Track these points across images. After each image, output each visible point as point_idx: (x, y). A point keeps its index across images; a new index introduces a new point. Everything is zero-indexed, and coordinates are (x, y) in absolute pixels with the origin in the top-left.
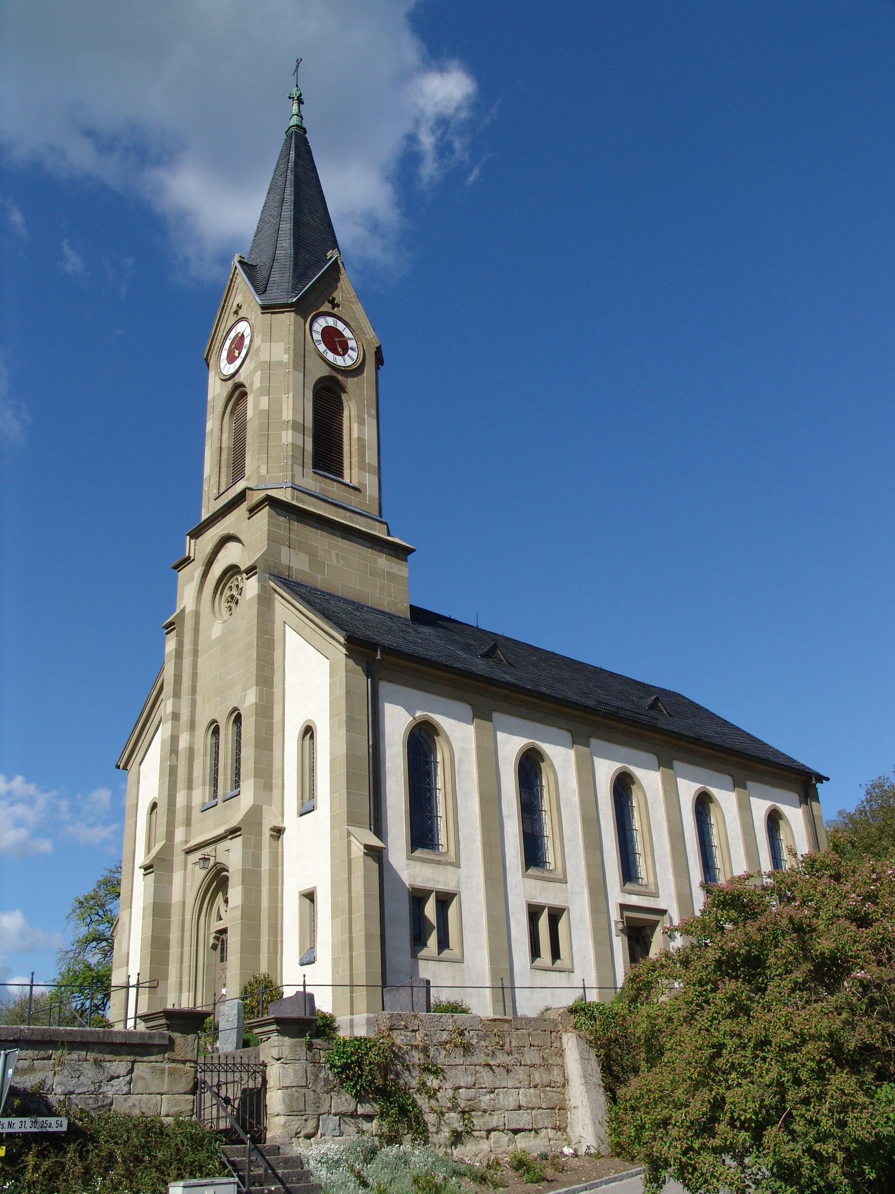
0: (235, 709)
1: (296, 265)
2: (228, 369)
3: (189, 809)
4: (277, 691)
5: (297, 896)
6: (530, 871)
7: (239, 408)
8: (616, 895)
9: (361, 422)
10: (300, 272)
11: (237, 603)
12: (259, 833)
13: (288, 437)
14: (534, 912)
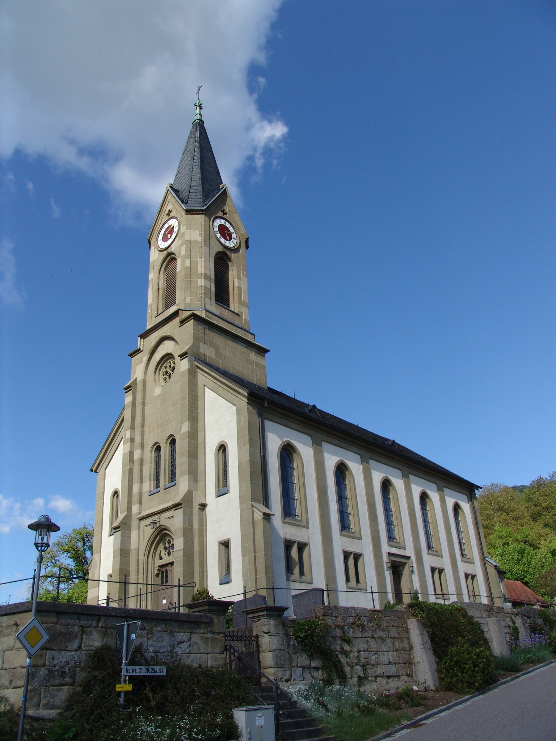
1: (203, 190)
2: (163, 245)
3: (141, 494)
4: (200, 424)
5: (217, 544)
6: (343, 533)
7: (170, 267)
8: (386, 548)
9: (239, 278)
10: (206, 195)
11: (170, 376)
12: (192, 508)
13: (201, 282)
14: (346, 555)
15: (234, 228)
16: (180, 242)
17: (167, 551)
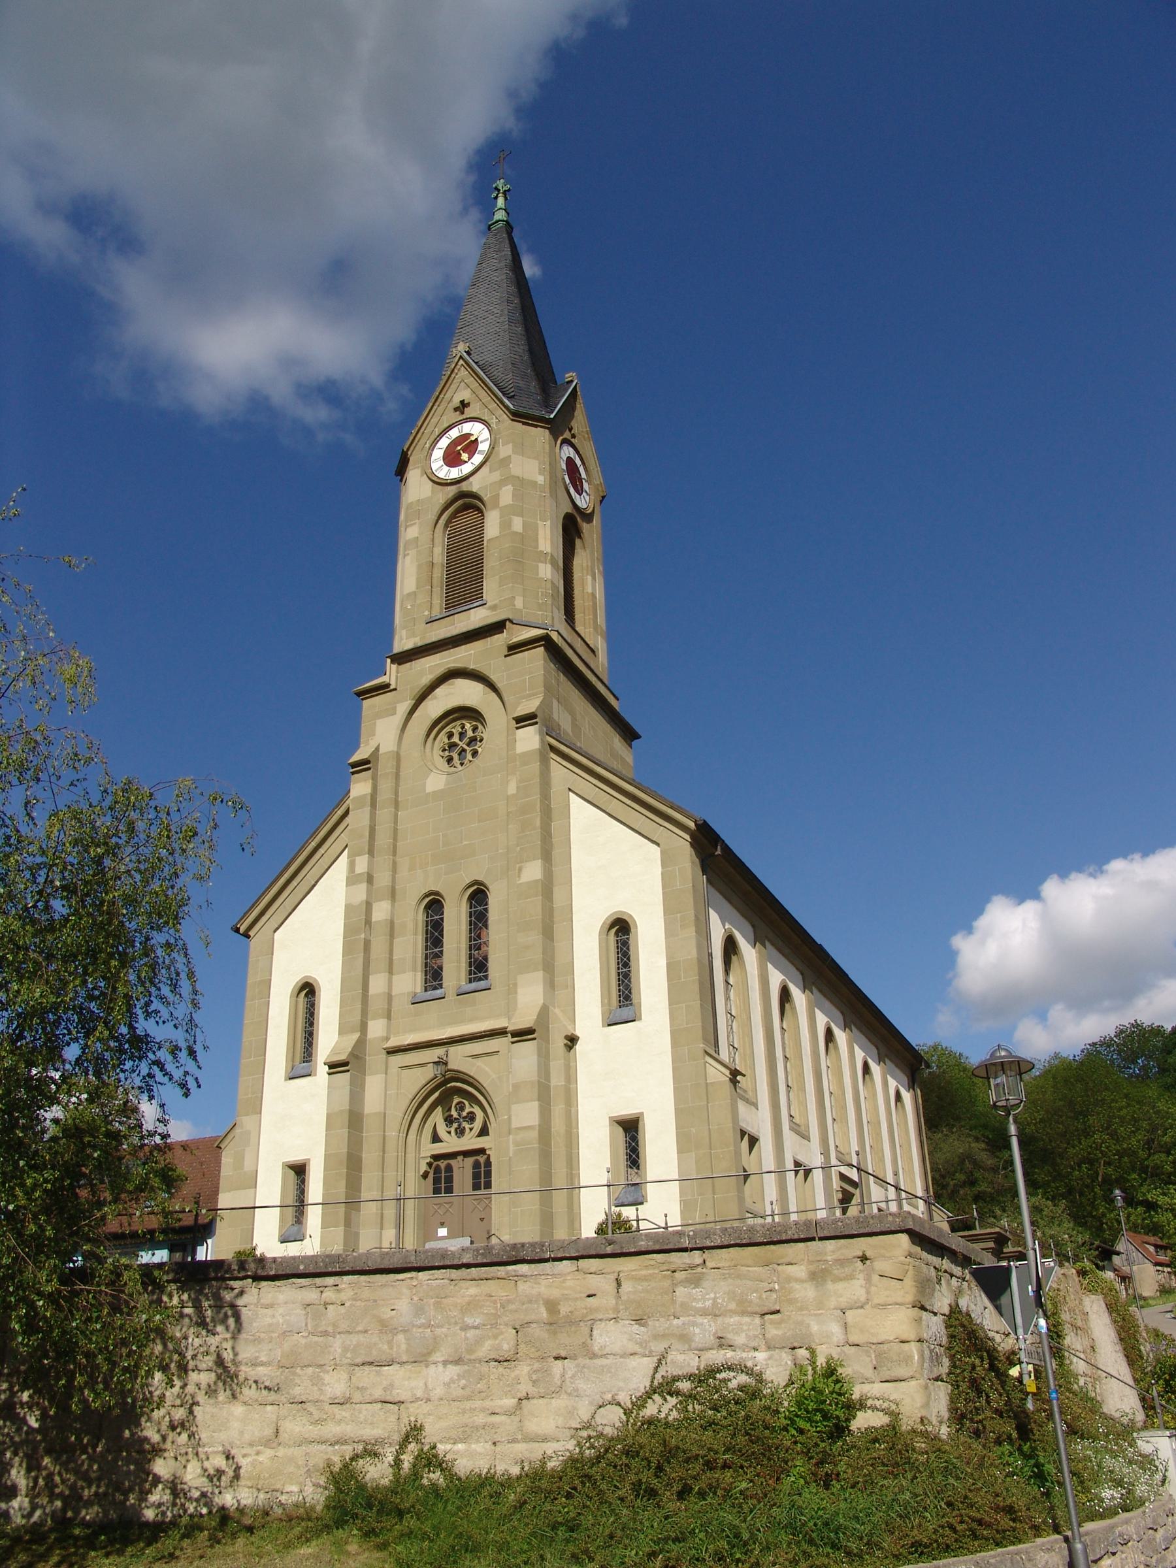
0: (476, 883)
15: (586, 470)
16: (496, 476)
17: (455, 1125)
